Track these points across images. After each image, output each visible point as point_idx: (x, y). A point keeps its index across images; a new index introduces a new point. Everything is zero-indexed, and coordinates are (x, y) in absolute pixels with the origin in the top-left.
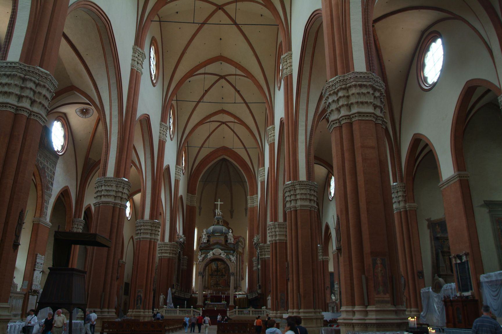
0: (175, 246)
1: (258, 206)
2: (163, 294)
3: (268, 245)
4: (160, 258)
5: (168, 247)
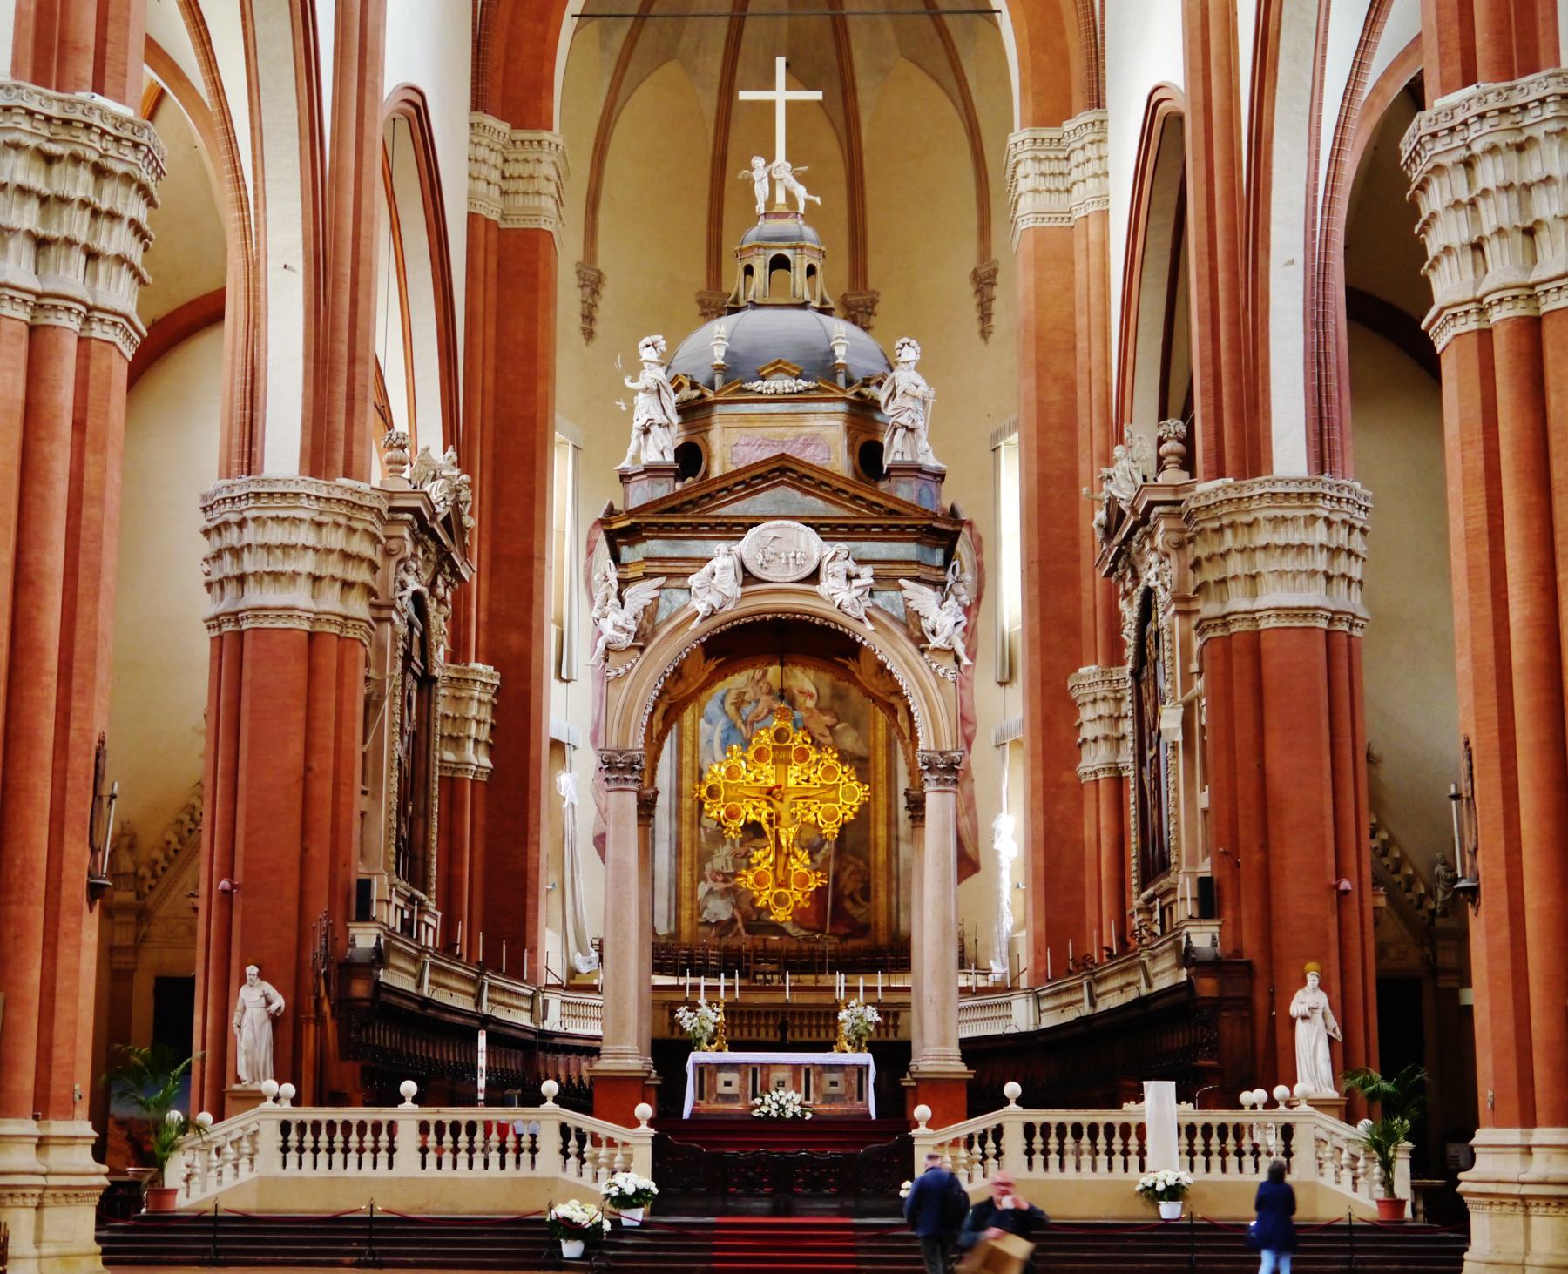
0: (369, 517)
1: (1104, 215)
2: (261, 976)
3: (1279, 489)
4: (228, 628)
5: (295, 521)
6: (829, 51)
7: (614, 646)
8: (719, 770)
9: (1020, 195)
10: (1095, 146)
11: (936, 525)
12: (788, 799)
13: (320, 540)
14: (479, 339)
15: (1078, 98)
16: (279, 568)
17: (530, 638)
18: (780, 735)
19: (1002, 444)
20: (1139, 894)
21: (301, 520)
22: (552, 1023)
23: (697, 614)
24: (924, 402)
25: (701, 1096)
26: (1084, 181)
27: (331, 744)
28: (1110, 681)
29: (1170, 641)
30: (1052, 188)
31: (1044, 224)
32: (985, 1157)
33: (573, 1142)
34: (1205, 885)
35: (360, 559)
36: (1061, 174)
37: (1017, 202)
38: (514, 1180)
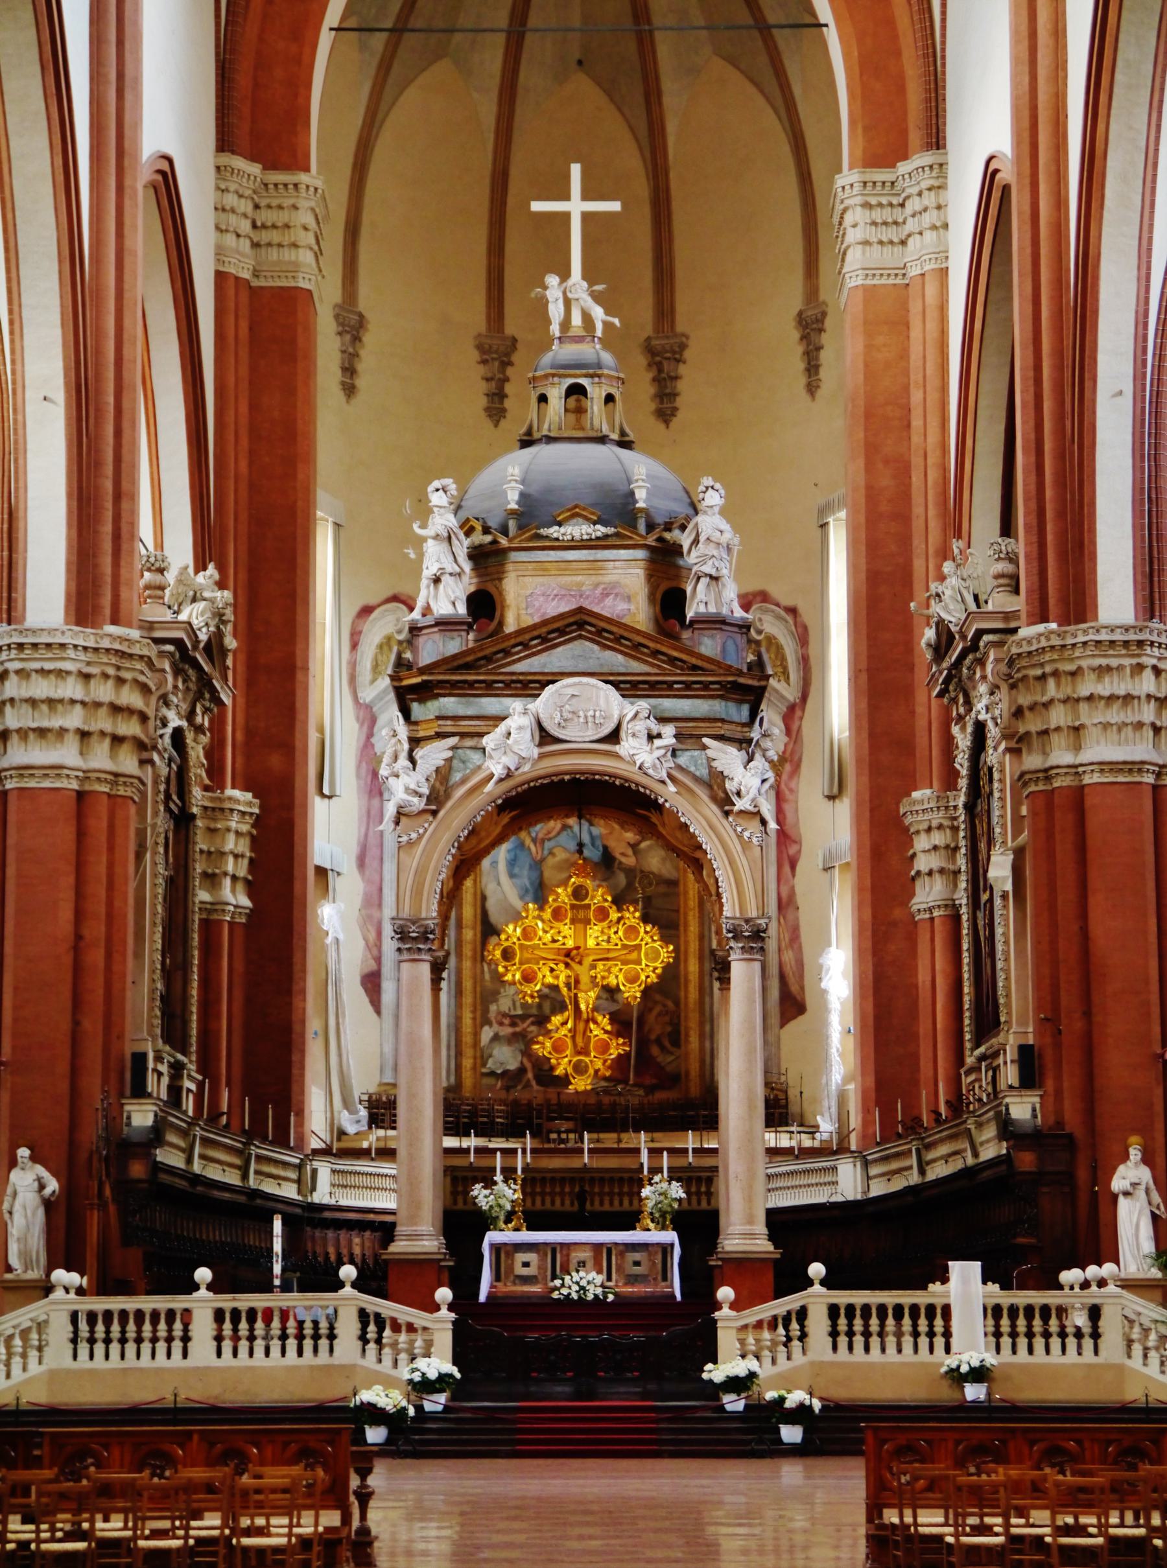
0: (139, 666)
1: (944, 273)
2: (34, 1158)
3: (1104, 636)
5: (61, 674)
6: (631, 47)
7: (406, 810)
8: (515, 930)
9: (848, 247)
10: (933, 193)
11: (741, 680)
12: (588, 961)
13: (88, 693)
14: (230, 418)
15: (915, 137)
16: (45, 724)
17: (293, 759)
18: (579, 893)
19: (831, 520)
20: (972, 1050)
21: (68, 673)
22: (322, 1195)
23: (492, 776)
24: (729, 549)
25: (497, 1277)
26: (921, 233)
27: (102, 910)
28: (947, 808)
29: (1000, 780)
30: (885, 239)
31: (875, 282)
32: (789, 1339)
33: (372, 1328)
34: (1027, 1056)
35: (129, 711)
36: (896, 223)
37: (845, 253)
38: (312, 1368)
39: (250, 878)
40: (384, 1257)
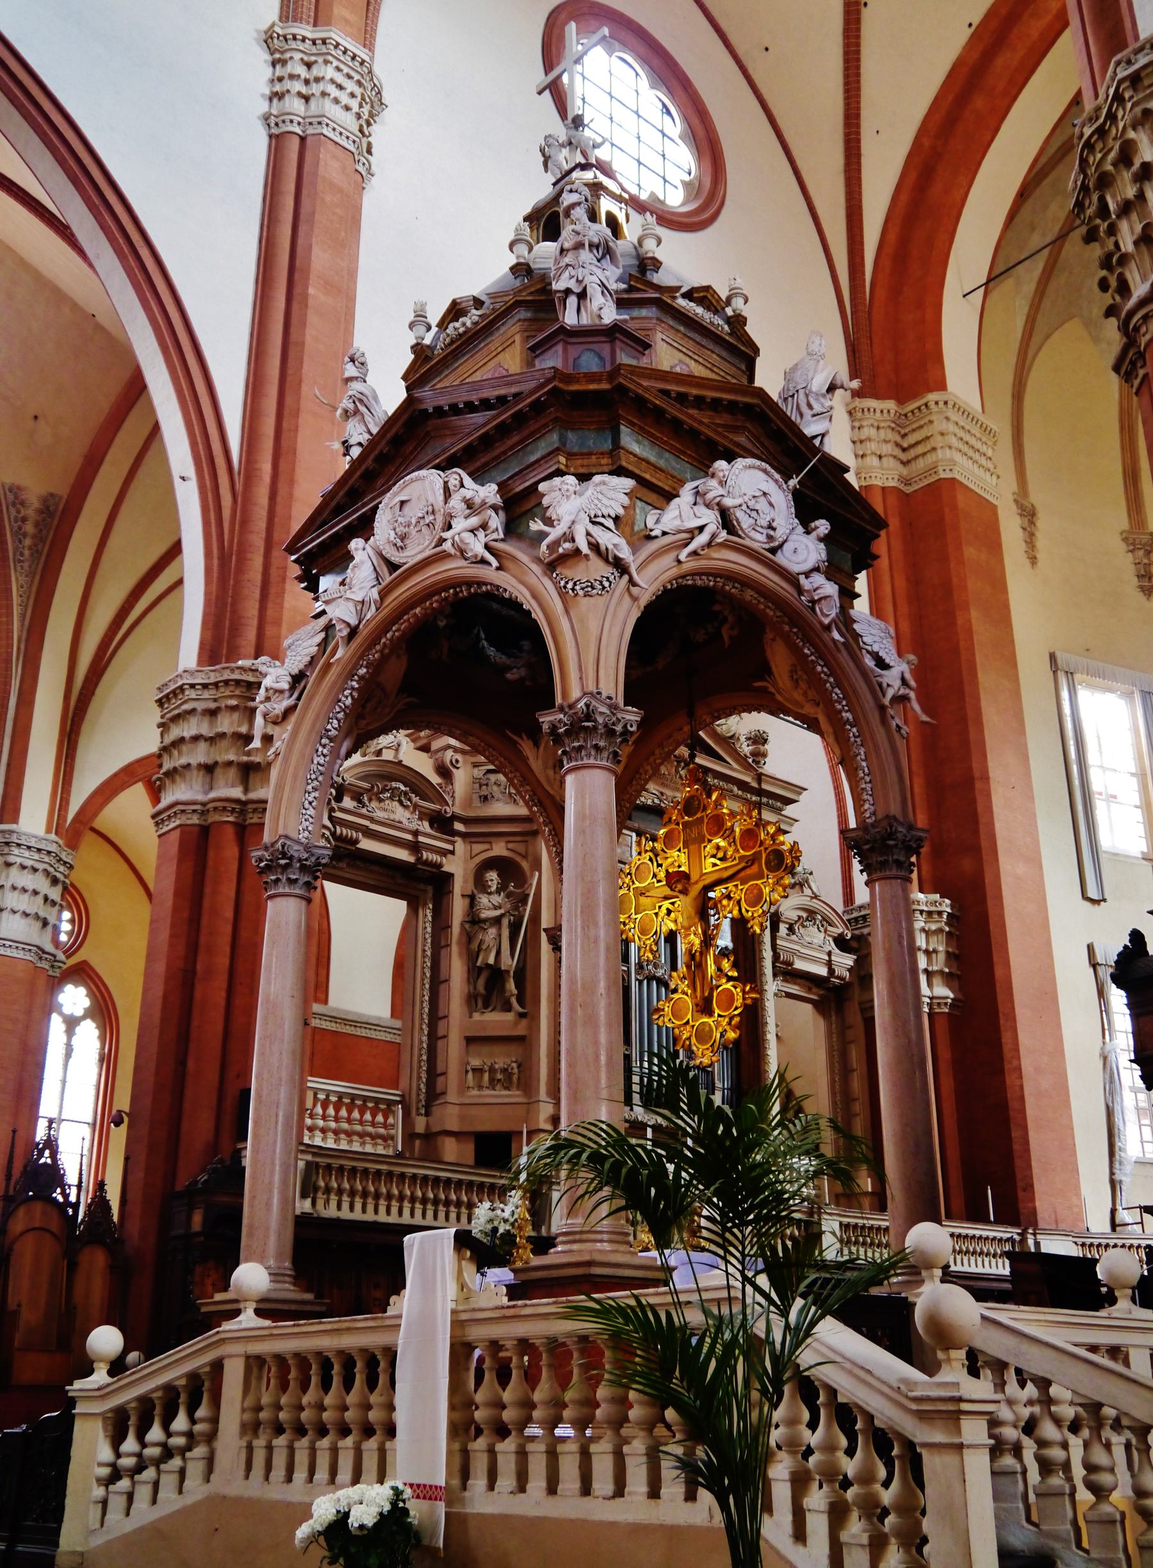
17: (981, 859)
39: (947, 970)
40: (204, 1309)
